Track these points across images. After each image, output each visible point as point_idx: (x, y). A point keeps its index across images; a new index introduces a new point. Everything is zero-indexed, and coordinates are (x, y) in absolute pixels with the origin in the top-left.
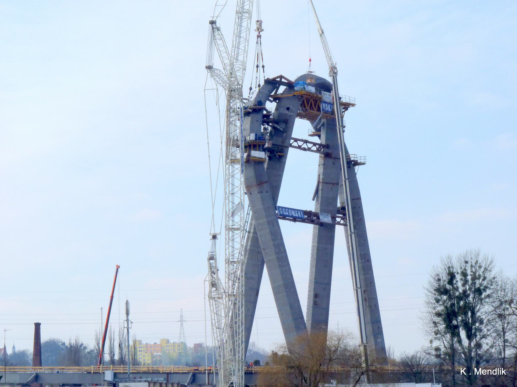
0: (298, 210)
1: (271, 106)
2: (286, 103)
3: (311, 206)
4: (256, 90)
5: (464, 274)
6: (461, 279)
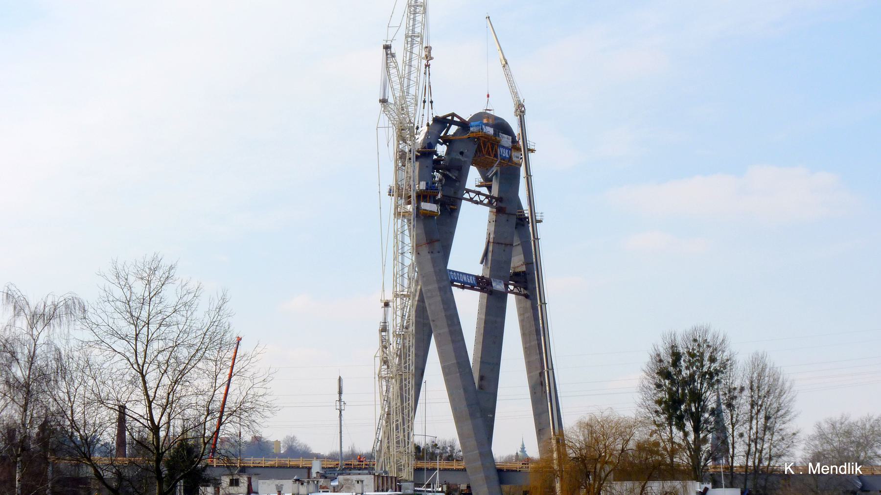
0: (470, 275)
1: (441, 150)
2: (460, 147)
3: (478, 270)
4: (424, 129)
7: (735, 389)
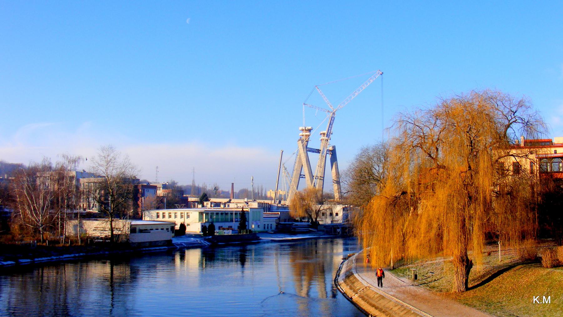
0: (314, 149)
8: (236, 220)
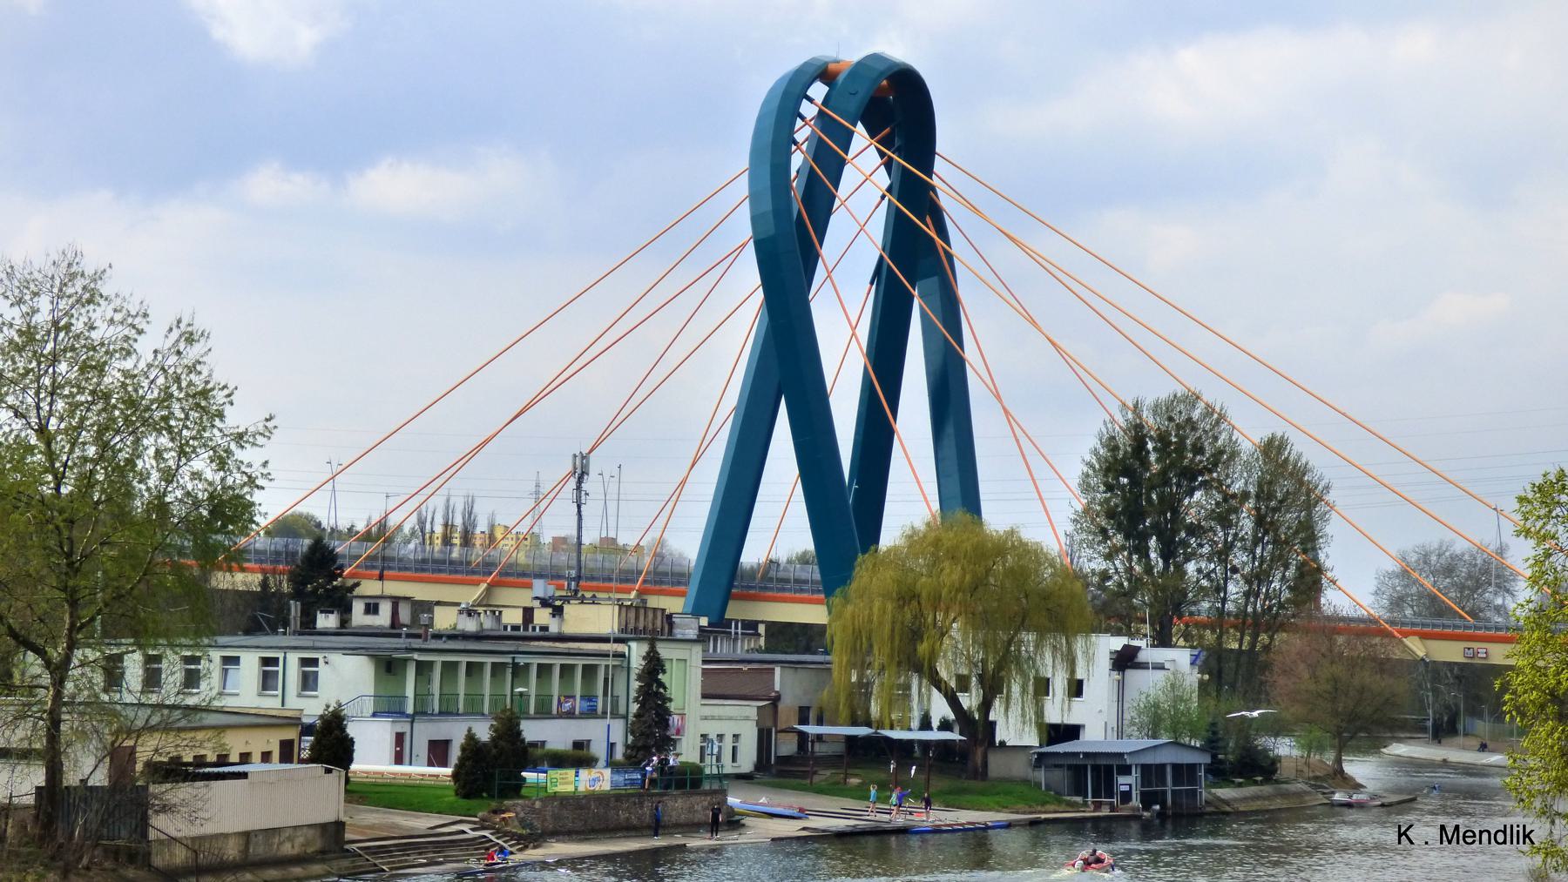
5: (1163, 438)
6: (1155, 449)
7: (1234, 496)
8: (567, 706)
